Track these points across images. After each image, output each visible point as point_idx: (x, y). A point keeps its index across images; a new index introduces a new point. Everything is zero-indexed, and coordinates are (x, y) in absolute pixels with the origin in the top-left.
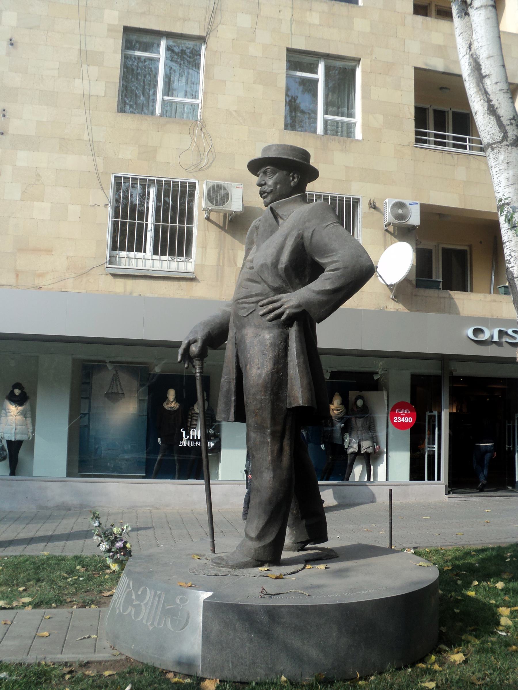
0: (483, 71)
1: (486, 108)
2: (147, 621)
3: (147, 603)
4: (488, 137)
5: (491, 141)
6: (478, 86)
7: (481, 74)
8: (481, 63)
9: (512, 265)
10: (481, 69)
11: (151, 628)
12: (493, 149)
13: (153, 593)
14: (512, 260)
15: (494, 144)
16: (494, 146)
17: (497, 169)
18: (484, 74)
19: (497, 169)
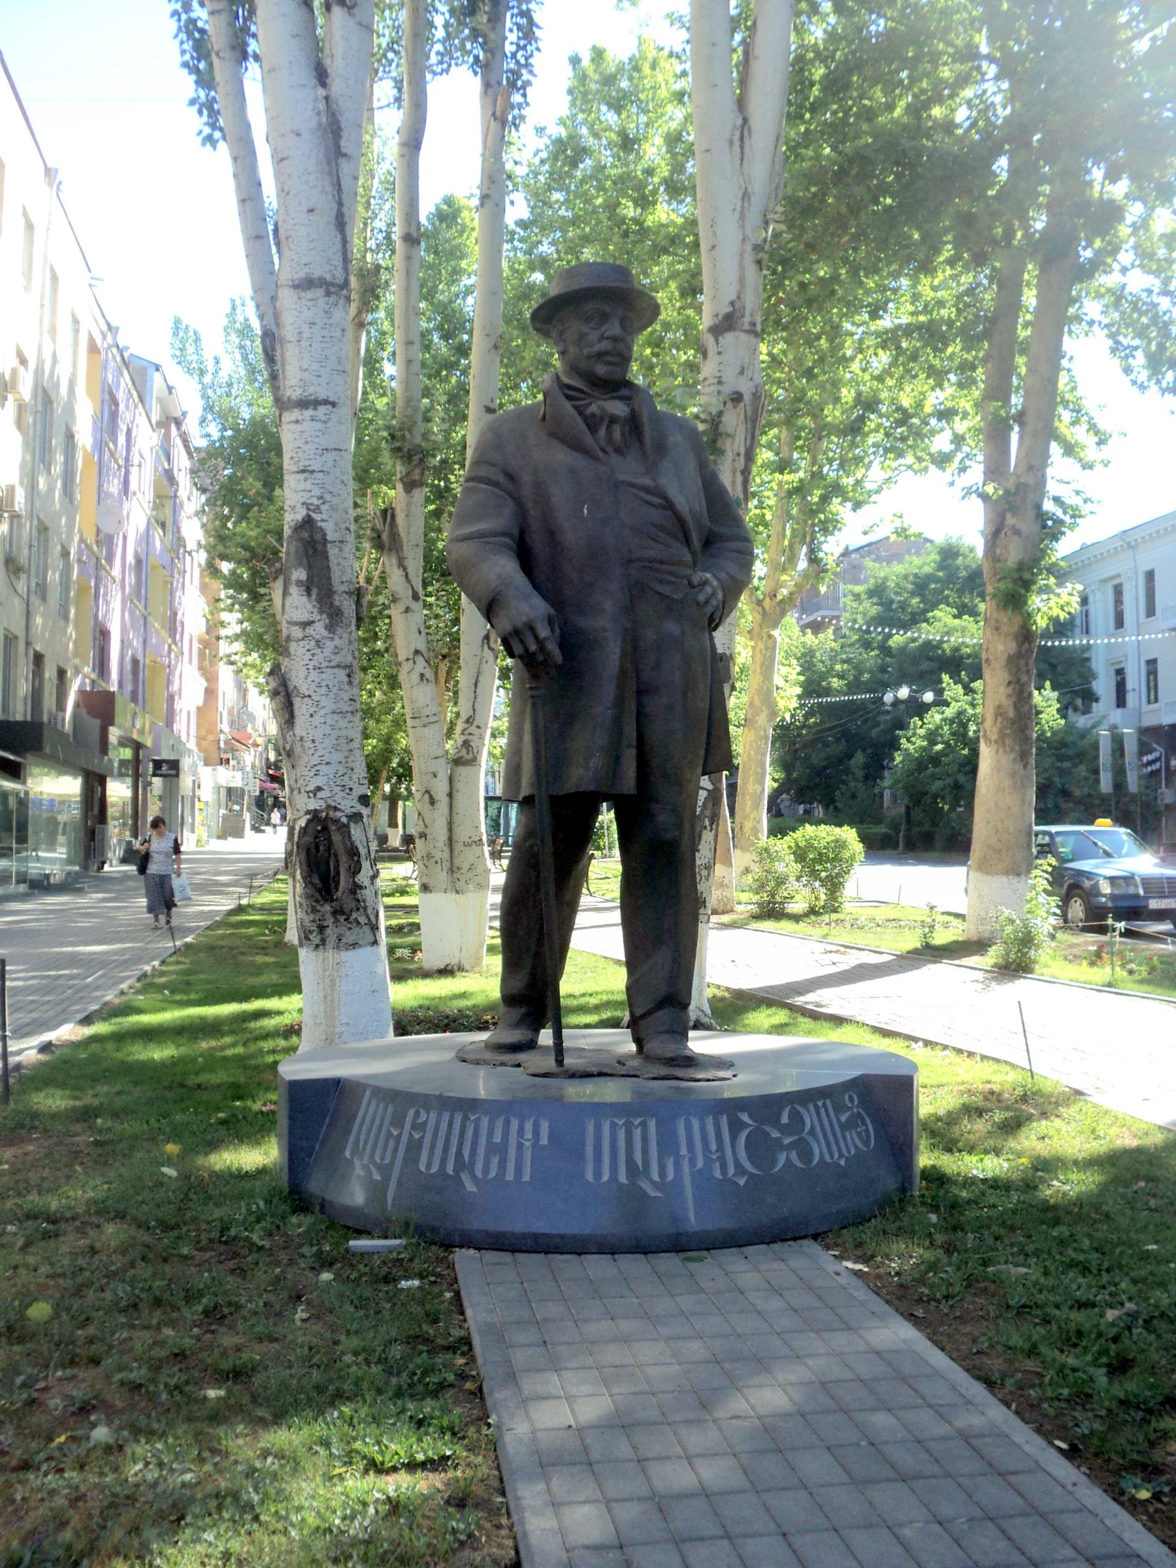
0: (342, 143)
1: (334, 212)
2: (832, 1156)
3: (813, 1128)
4: (327, 268)
5: (328, 277)
6: (329, 163)
7: (338, 147)
8: (344, 124)
9: (324, 516)
10: (340, 137)
11: (842, 1162)
12: (328, 294)
13: (812, 1108)
14: (324, 508)
15: (333, 285)
16: (332, 289)
17: (326, 333)
18: (344, 150)
19: (326, 333)
